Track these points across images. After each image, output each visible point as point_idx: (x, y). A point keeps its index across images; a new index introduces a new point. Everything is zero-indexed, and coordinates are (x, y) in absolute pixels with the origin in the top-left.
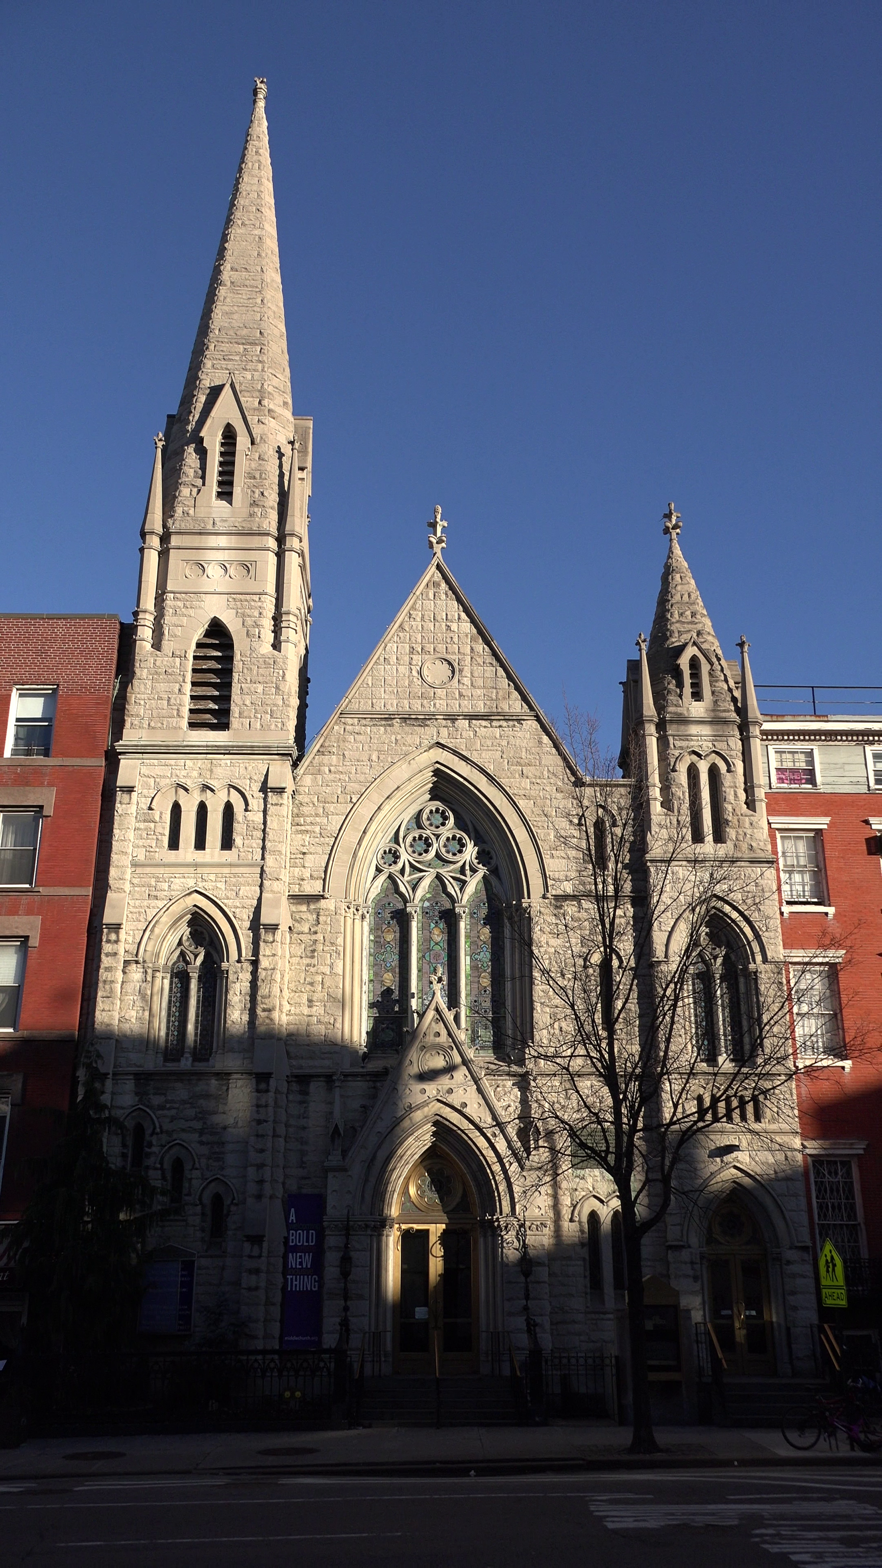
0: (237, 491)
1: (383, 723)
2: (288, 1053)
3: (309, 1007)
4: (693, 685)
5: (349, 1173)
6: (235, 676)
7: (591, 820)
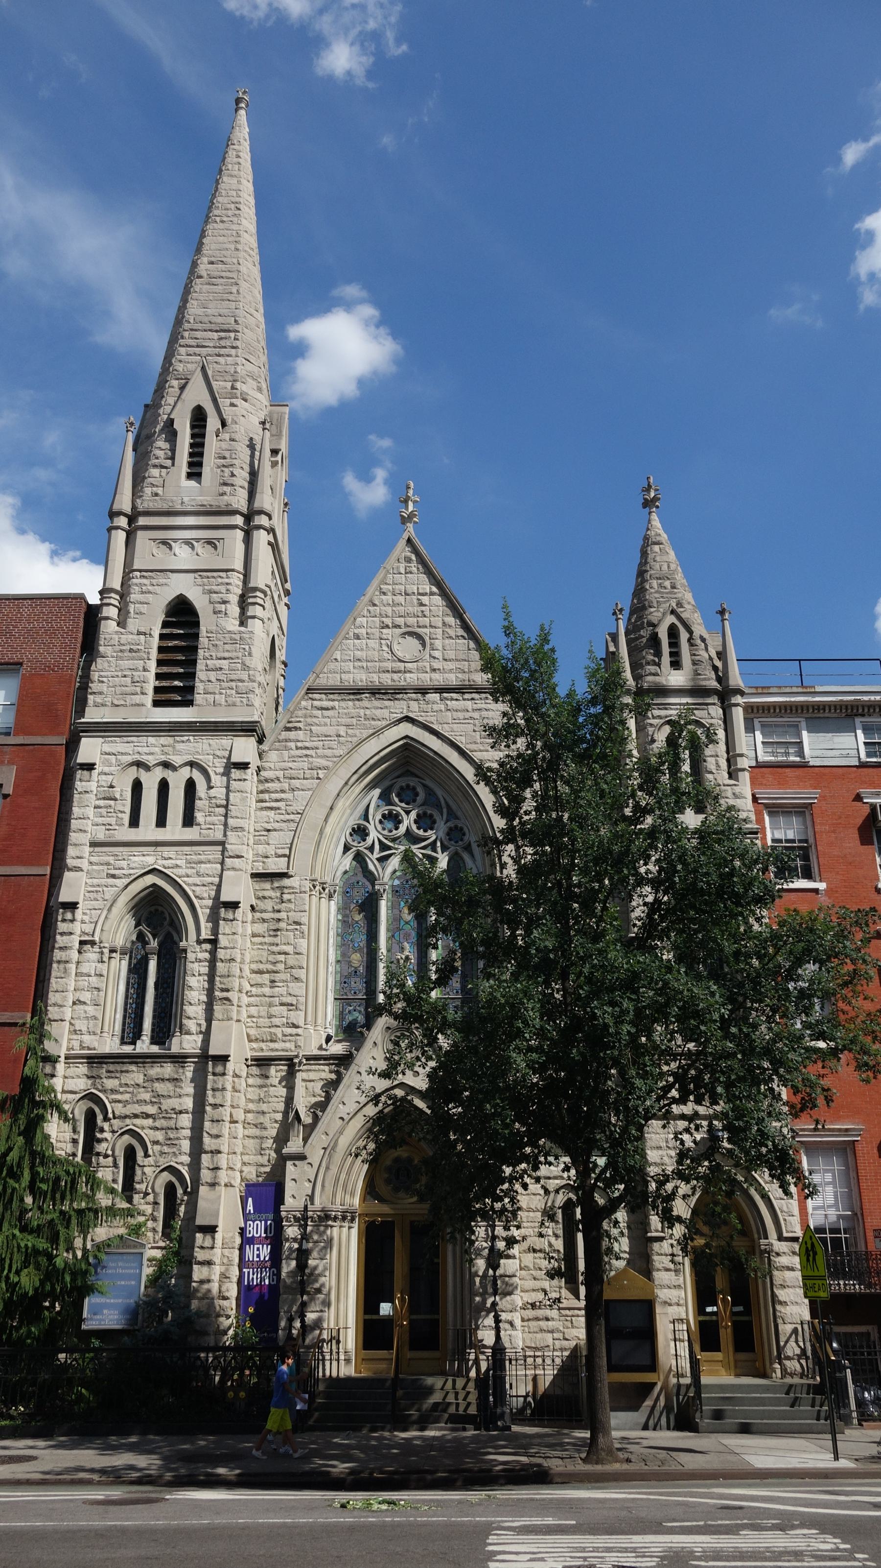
0: (206, 470)
1: (352, 697)
2: (248, 1035)
3: (271, 987)
4: (672, 654)
5: (309, 1161)
6: (201, 652)
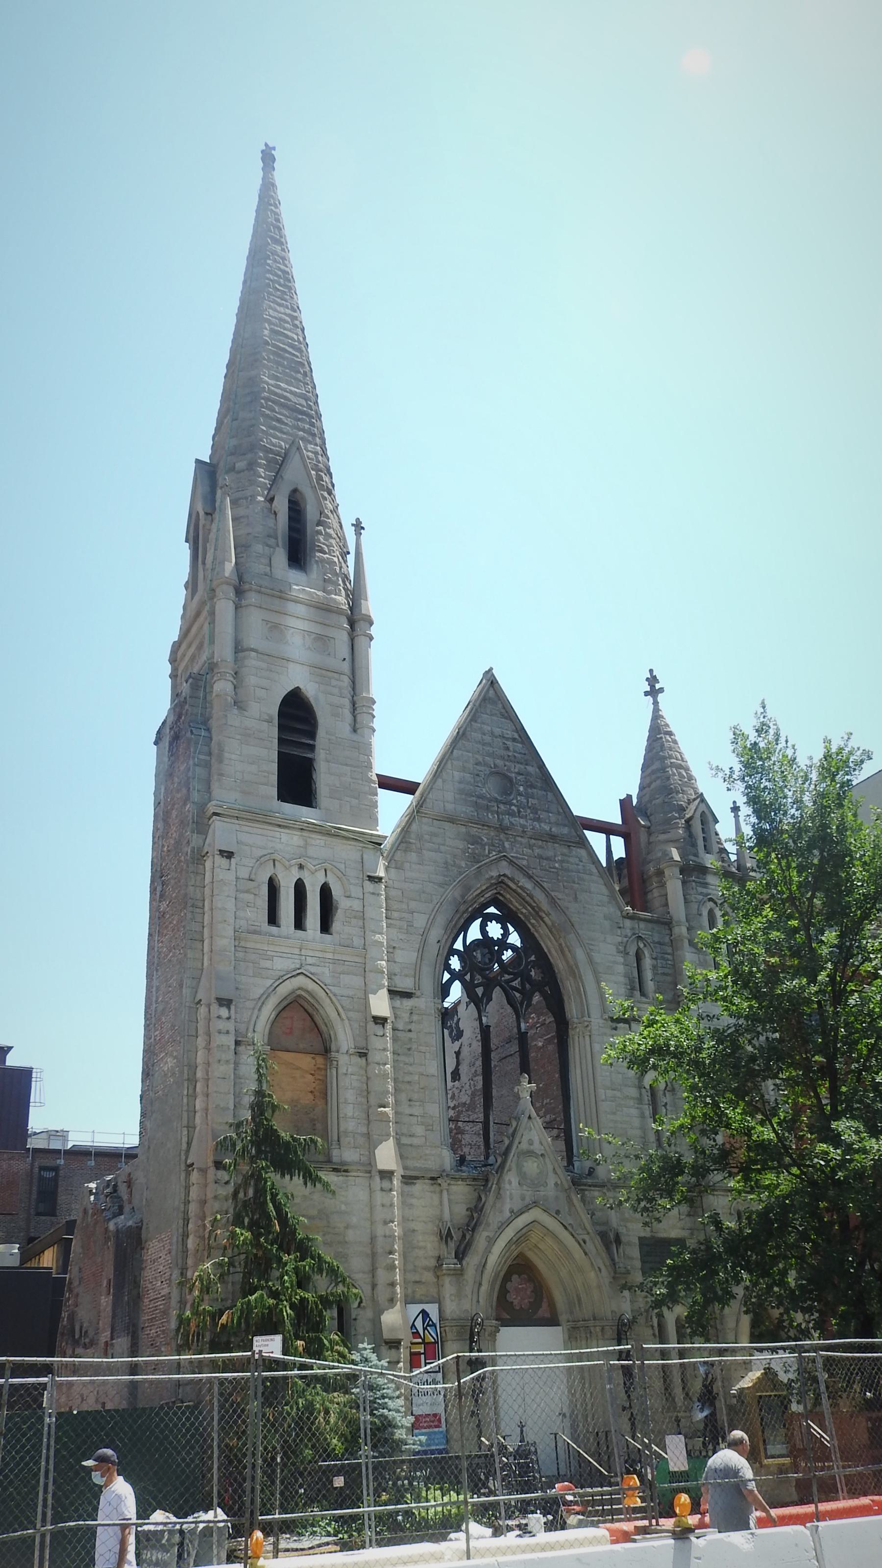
7: (632, 951)
